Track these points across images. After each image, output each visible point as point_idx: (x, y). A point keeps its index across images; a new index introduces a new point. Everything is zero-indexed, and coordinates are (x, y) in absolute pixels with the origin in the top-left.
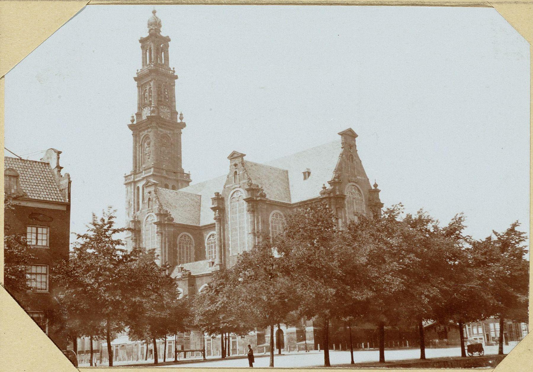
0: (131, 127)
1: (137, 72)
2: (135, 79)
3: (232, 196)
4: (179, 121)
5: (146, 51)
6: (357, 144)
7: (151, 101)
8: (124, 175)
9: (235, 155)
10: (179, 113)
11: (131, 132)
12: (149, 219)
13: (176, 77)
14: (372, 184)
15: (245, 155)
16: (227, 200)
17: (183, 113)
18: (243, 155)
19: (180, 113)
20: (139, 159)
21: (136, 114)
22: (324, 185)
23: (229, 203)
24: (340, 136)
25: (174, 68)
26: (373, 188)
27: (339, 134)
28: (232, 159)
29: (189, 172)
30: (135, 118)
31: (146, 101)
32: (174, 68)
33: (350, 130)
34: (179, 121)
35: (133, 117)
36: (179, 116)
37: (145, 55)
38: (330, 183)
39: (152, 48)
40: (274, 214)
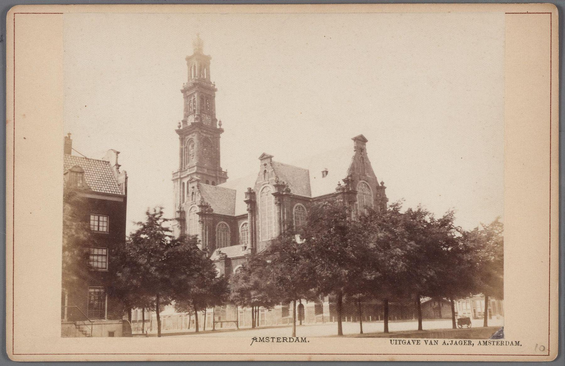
0: (179, 132)
1: (183, 85)
3: (262, 190)
5: (191, 68)
7: (194, 110)
9: (265, 157)
11: (178, 136)
12: (192, 210)
13: (216, 90)
14: (379, 182)
15: (273, 157)
17: (221, 120)
18: (271, 157)
19: (219, 120)
20: (185, 159)
25: (214, 82)
26: (380, 185)
28: (262, 159)
29: (227, 170)
30: (182, 124)
31: (191, 110)
32: (214, 82)
33: (362, 136)
34: (218, 127)
35: (180, 123)
36: (218, 123)
37: (190, 72)
38: (344, 180)
39: (196, 66)
40: (297, 206)
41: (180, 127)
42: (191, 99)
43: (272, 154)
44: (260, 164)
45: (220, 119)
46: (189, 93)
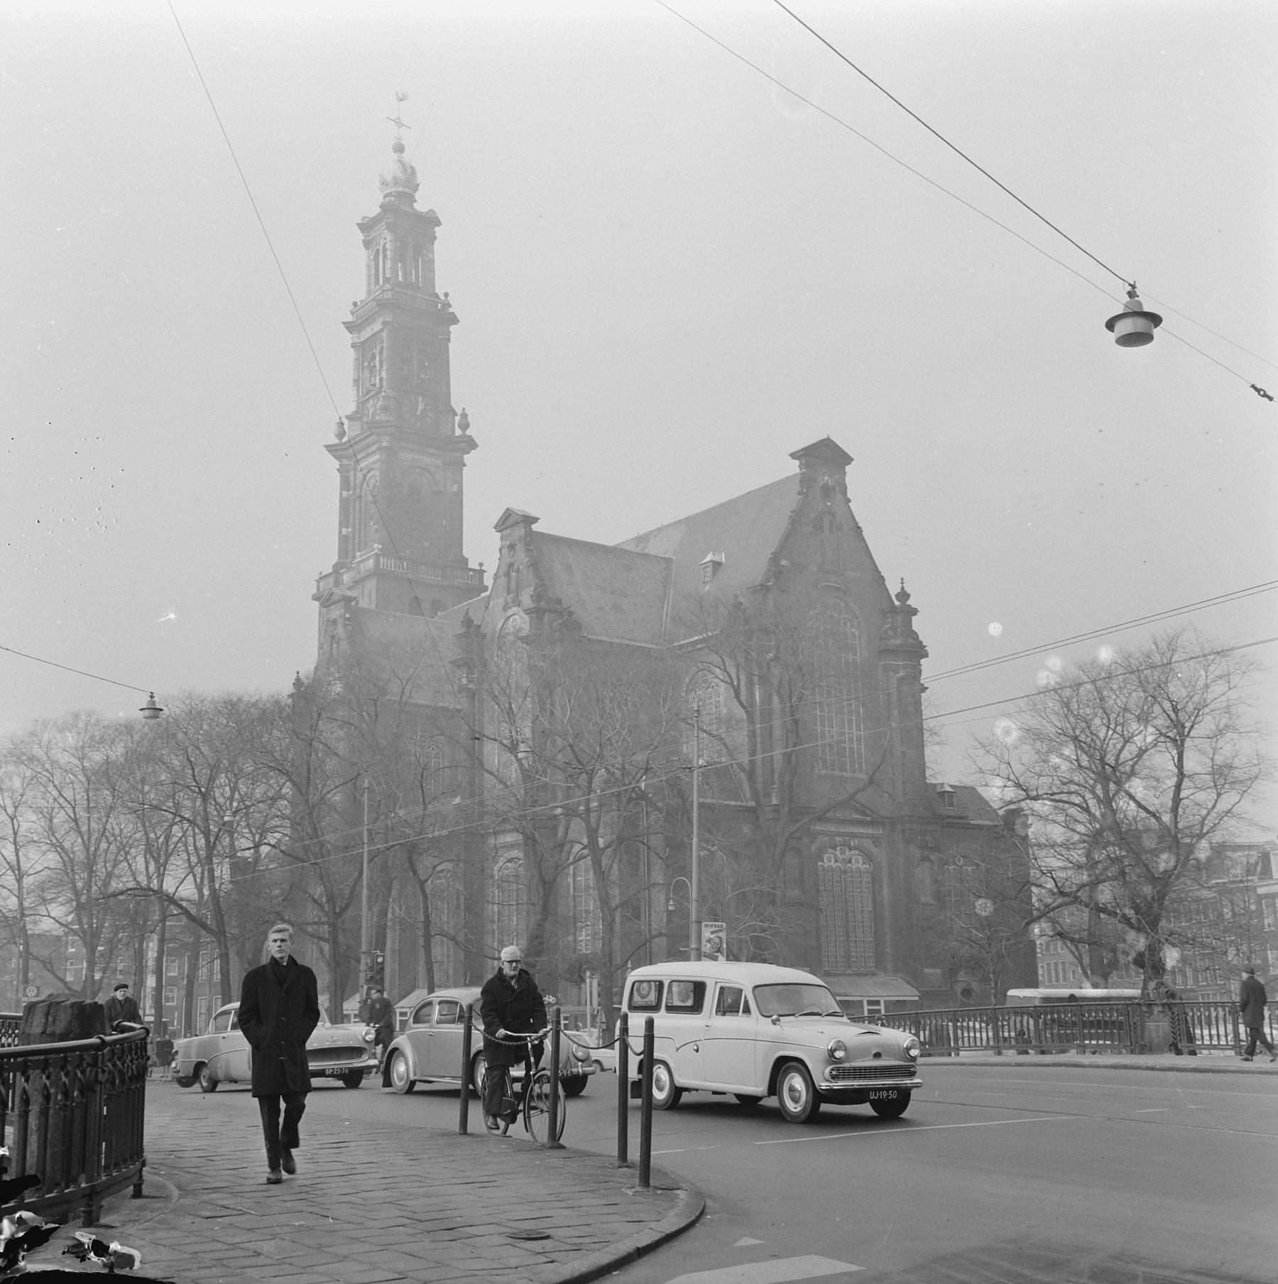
2: (350, 327)
4: (458, 432)
8: (317, 577)
9: (511, 520)
10: (459, 411)
11: (336, 464)
13: (454, 320)
14: (893, 589)
15: (536, 520)
17: (467, 412)
18: (530, 520)
21: (348, 418)
24: (797, 462)
25: (446, 295)
26: (897, 603)
27: (794, 456)
36: (457, 419)
37: (373, 263)
41: (341, 434)
42: (375, 351)
43: (534, 514)
44: (499, 543)
45: (464, 409)
46: (367, 333)
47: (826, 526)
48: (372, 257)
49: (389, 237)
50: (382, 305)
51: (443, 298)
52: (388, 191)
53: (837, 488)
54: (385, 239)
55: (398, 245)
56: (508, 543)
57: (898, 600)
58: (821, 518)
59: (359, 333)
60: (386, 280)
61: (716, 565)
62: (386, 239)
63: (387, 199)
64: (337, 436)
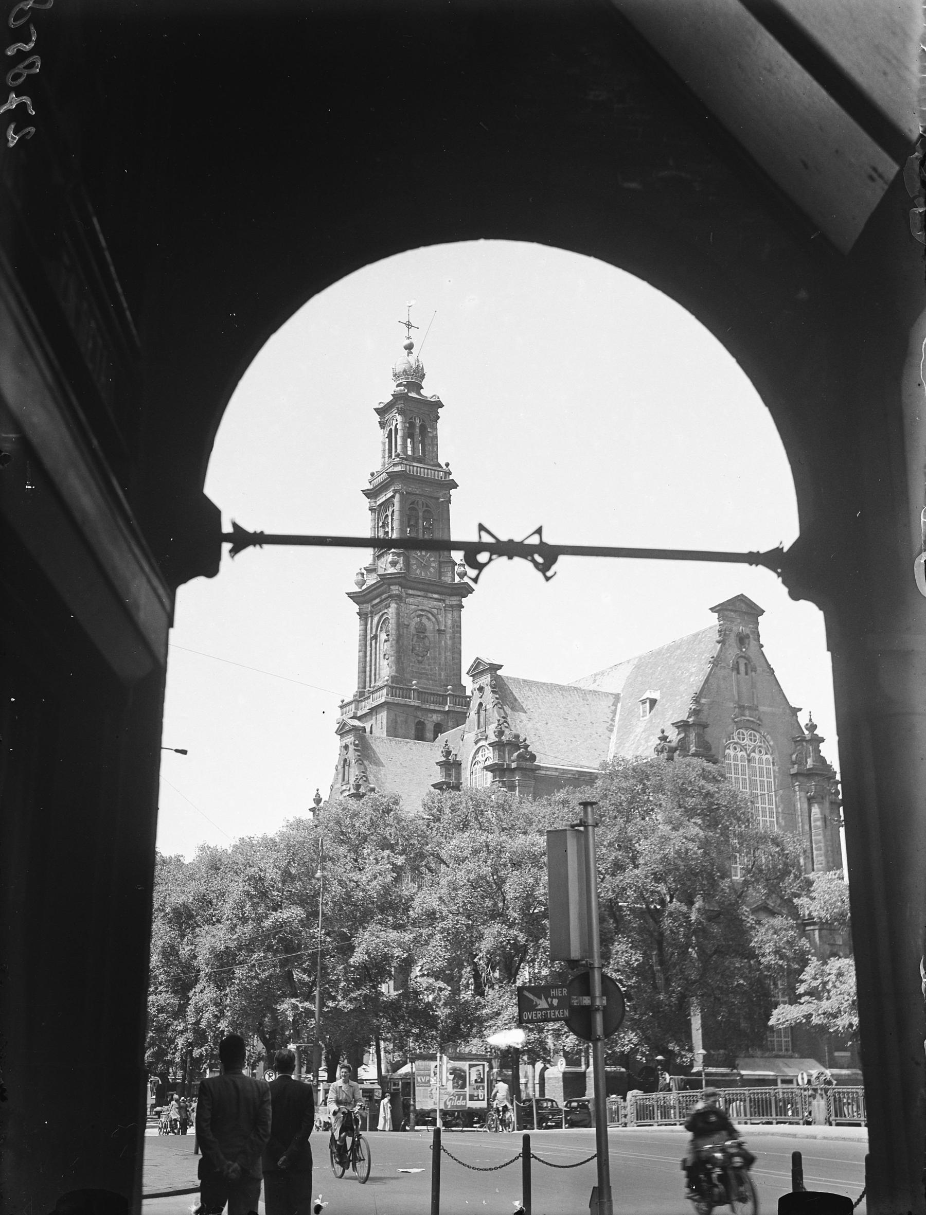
2: (369, 494)
6: (761, 629)
11: (356, 608)
13: (455, 486)
14: (803, 719)
15: (500, 667)
16: (466, 768)
22: (663, 732)
23: (468, 773)
25: (447, 465)
26: (806, 732)
27: (712, 609)
33: (741, 599)
34: (457, 579)
37: (387, 440)
38: (677, 725)
47: (742, 668)
48: (386, 436)
49: (399, 418)
50: (393, 477)
51: (444, 467)
52: (398, 382)
53: (751, 636)
54: (397, 421)
55: (408, 425)
56: (478, 687)
57: (807, 729)
58: (737, 662)
59: (376, 498)
60: (398, 456)
61: (653, 702)
62: (398, 420)
63: (398, 389)
64: (357, 583)
